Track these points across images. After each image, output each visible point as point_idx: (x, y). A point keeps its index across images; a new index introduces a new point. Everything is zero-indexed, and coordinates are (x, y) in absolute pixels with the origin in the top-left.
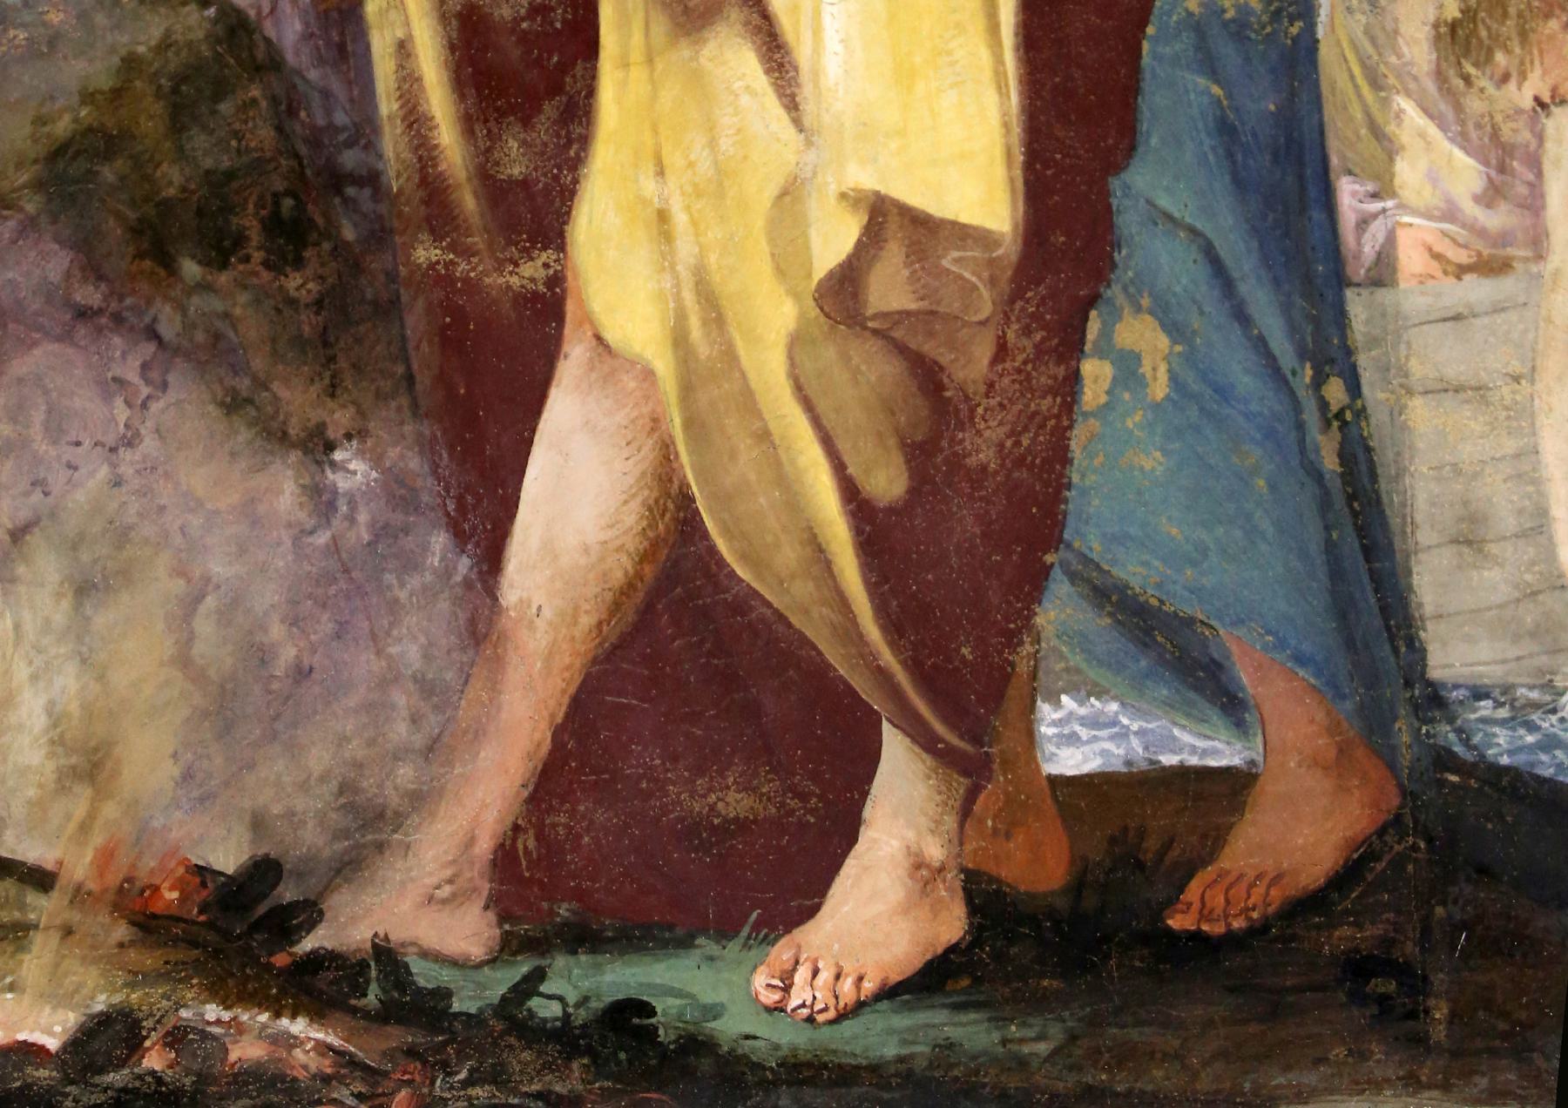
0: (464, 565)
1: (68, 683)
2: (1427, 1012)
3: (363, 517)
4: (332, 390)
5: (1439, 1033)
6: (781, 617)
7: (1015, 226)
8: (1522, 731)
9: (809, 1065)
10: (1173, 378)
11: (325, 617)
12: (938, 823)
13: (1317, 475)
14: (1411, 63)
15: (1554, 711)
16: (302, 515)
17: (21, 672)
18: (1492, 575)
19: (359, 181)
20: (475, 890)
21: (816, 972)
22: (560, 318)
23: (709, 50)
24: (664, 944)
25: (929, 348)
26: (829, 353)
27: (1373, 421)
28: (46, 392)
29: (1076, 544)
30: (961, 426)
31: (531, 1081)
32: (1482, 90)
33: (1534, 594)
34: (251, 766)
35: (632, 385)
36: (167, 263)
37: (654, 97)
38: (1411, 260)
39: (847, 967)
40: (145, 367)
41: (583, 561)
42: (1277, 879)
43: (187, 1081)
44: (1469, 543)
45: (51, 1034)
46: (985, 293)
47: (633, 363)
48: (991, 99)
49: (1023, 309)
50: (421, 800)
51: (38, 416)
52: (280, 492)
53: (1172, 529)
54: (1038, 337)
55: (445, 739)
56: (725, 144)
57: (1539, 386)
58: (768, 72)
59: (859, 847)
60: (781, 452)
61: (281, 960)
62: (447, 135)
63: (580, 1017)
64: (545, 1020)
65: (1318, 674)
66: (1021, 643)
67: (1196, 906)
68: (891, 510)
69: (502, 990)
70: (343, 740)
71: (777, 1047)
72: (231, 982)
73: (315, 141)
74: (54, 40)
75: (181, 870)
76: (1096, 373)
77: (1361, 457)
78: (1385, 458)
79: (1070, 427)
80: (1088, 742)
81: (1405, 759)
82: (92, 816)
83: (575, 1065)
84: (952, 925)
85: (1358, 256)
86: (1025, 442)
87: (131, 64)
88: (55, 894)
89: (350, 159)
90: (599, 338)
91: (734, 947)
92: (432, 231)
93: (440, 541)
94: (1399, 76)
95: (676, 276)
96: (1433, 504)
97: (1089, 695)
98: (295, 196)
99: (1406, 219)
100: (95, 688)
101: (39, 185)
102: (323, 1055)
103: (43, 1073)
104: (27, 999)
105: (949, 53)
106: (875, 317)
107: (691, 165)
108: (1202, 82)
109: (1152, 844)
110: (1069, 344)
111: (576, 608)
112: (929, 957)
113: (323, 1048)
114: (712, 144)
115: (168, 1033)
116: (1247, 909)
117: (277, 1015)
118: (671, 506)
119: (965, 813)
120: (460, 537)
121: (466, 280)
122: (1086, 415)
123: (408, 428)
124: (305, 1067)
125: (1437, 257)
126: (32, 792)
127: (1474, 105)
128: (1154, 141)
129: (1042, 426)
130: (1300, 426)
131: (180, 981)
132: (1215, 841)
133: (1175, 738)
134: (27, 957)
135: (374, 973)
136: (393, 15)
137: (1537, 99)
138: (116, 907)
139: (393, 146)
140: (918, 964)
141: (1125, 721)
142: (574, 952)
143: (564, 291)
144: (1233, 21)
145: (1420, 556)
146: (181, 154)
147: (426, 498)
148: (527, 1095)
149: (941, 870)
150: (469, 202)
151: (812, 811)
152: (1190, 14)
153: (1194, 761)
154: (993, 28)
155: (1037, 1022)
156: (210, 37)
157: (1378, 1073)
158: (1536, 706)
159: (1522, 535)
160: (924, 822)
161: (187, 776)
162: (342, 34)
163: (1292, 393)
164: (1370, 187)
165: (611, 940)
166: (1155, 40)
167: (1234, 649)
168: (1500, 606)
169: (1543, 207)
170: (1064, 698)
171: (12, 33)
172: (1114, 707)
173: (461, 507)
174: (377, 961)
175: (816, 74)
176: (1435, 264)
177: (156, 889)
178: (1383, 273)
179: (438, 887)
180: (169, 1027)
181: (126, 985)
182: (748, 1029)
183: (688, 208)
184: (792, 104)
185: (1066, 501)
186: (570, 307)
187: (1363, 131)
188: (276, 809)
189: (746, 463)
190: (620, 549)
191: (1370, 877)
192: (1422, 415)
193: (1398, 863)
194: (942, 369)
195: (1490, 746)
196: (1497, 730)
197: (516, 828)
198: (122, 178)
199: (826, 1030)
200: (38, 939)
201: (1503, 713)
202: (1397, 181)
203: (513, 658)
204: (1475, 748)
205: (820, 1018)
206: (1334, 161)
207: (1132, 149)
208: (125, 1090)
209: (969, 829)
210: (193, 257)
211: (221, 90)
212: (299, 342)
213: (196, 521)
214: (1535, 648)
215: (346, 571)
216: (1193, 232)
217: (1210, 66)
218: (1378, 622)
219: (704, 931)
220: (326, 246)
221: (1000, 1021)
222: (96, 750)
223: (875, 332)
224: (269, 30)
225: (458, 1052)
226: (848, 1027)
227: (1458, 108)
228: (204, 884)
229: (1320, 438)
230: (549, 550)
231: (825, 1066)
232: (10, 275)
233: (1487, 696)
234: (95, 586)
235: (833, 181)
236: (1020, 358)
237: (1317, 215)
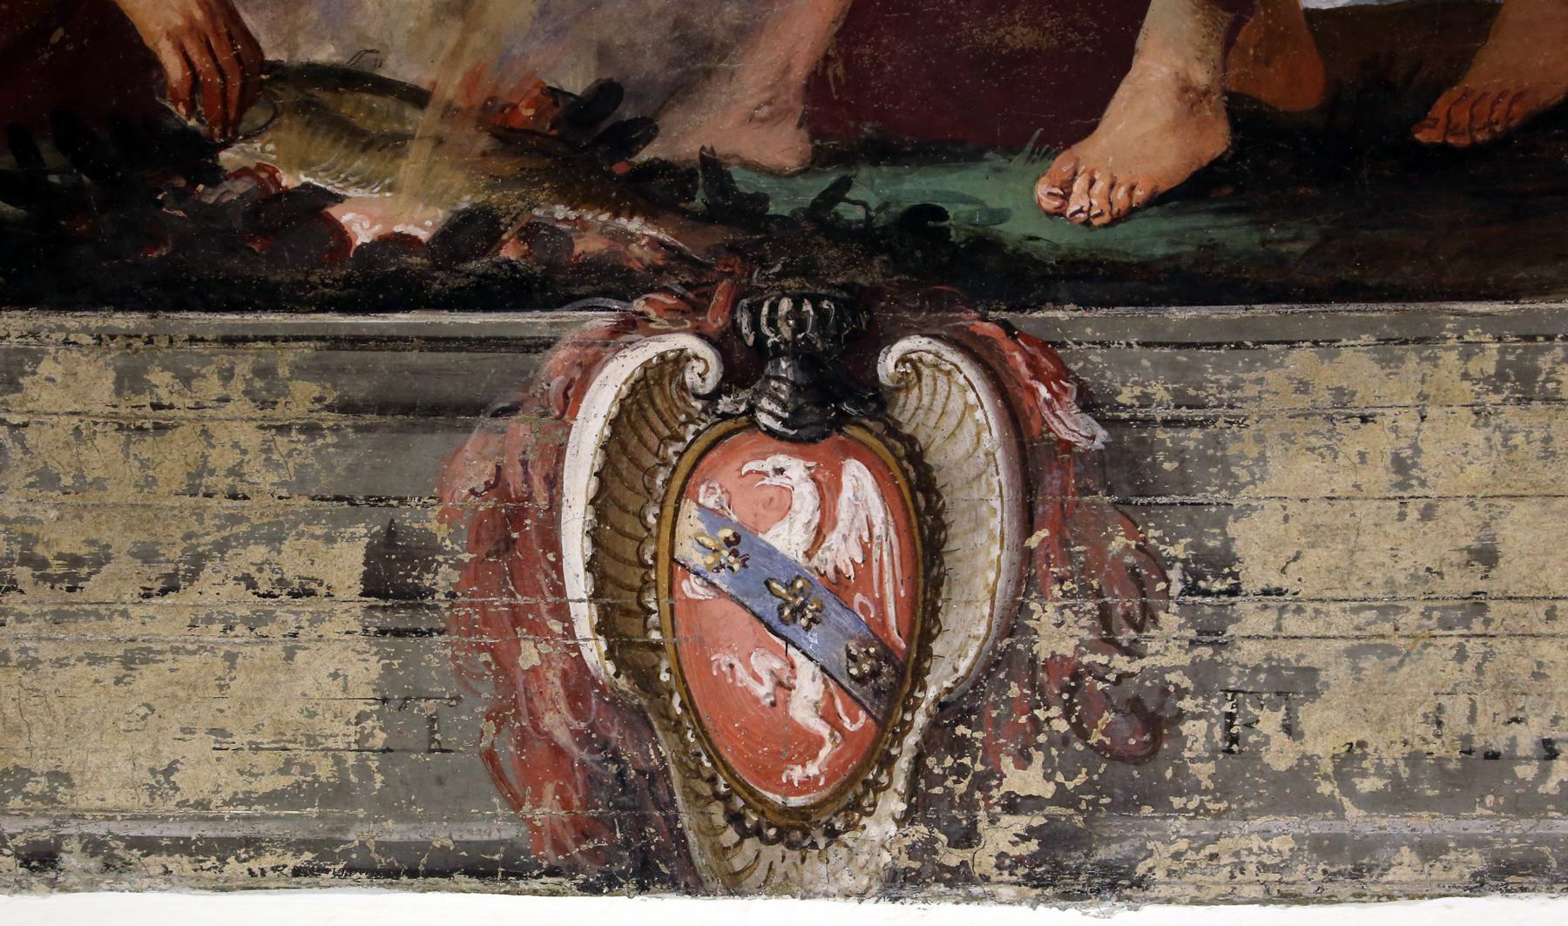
9: (1085, 262)
12: (1204, 52)
20: (789, 111)
21: (1092, 182)
24: (956, 158)
31: (837, 275)
39: (1121, 177)
42: (1519, 96)
43: (538, 269)
45: (423, 227)
50: (744, 33)
59: (1133, 73)
61: (620, 168)
63: (882, 219)
64: (850, 222)
67: (1443, 121)
69: (812, 196)
71: (1057, 247)
75: (537, 92)
82: (461, 44)
83: (876, 262)
84: (1215, 141)
88: (429, 111)
91: (1018, 161)
102: (655, 250)
103: (416, 260)
104: (403, 198)
112: (1195, 168)
113: (656, 244)
115: (523, 229)
116: (1490, 124)
117: (616, 215)
119: (1229, 43)
124: (640, 260)
131: (534, 184)
134: (404, 163)
135: (701, 181)
140: (1184, 175)
142: (876, 164)
148: (834, 286)
149: (1206, 93)
160: (1190, 51)
174: (704, 170)
177: (515, 107)
179: (759, 108)
180: (523, 223)
181: (487, 187)
182: (1031, 231)
188: (619, 41)
197: (827, 58)
199: (1102, 233)
200: (414, 148)
205: (1096, 222)
208: (485, 276)
209: (1232, 59)
225: (773, 249)
226: (1122, 229)
228: (556, 104)
231: (1100, 264)
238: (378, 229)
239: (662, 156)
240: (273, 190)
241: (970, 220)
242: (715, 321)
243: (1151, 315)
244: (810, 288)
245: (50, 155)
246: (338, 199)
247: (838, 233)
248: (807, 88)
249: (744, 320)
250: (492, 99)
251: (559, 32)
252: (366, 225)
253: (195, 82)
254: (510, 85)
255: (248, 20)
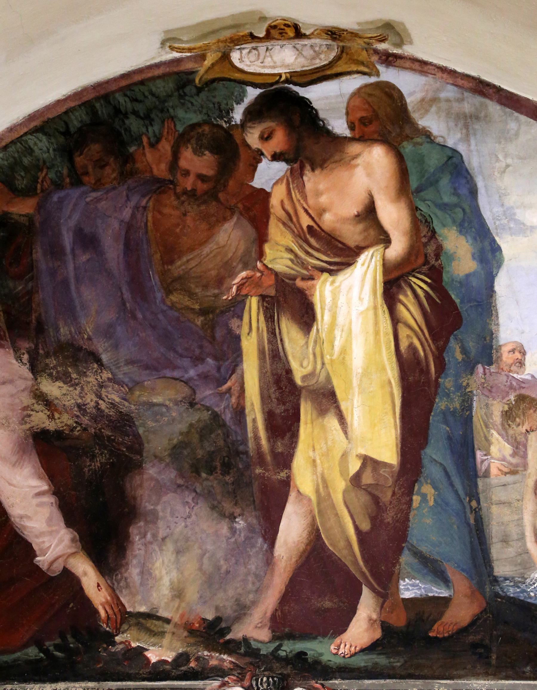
0: (266, 546)
1: (174, 574)
2: (491, 657)
3: (242, 535)
4: (236, 504)
5: (494, 662)
6: (339, 559)
7: (398, 463)
8: (516, 588)
9: (343, 668)
10: (435, 500)
11: (233, 559)
12: (375, 609)
13: (468, 524)
14: (495, 422)
15: (524, 583)
16: (228, 534)
17: (164, 572)
18: (510, 549)
19: (243, 453)
20: (266, 625)
21: (345, 645)
22: (289, 486)
23: (326, 419)
25: (377, 493)
26: (353, 494)
27: (483, 511)
28: (170, 505)
29: (410, 541)
30: (383, 513)
32: (513, 428)
33: (521, 554)
34: (215, 594)
35: (306, 502)
36: (198, 473)
37: (313, 432)
38: (494, 471)
39: (353, 644)
40: (193, 499)
41: (293, 545)
42: (456, 624)
43: (200, 669)
44: (505, 542)
45: (169, 657)
46: (391, 479)
47: (306, 497)
48: (393, 431)
49: (399, 483)
50: (254, 603)
51: (169, 510)
52: (223, 529)
53: (434, 538)
54: (403, 490)
55: (260, 588)
56: (329, 443)
57: (524, 502)
58: (340, 425)
59: (356, 615)
60: (341, 519)
61: (221, 641)
62: (264, 442)
63: (290, 655)
64: (282, 656)
65: (467, 573)
66: (396, 566)
67: (436, 630)
68: (366, 533)
70: (236, 588)
71: (336, 663)
72: (210, 646)
73: (233, 443)
74: (174, 420)
75: (199, 619)
76: (416, 499)
77: (480, 520)
78: (485, 520)
79: (410, 512)
80: (412, 590)
81: (488, 595)
82: (179, 606)
83: (289, 667)
84: (378, 634)
85: (481, 470)
86: (399, 516)
87: (191, 425)
88: (171, 625)
89: (241, 448)
90: (298, 491)
91: (326, 639)
92: (260, 466)
93: (260, 540)
94: (492, 425)
95: (317, 476)
96: (497, 532)
97: (412, 579)
98: (228, 457)
99: (493, 461)
100: (180, 576)
101: (170, 455)
102: (230, 664)
103: (168, 667)
104: (164, 649)
105: (383, 420)
106: (363, 486)
107: (321, 448)
108: (444, 426)
109: (426, 615)
110: (410, 492)
111: (291, 557)
112: (372, 642)
113: (231, 662)
114: (326, 443)
116: (448, 632)
117: (220, 654)
118: (314, 532)
119: (382, 607)
120: (265, 539)
121: (268, 477)
122: (413, 509)
123: (253, 513)
124: (227, 667)
125: (500, 470)
126: (166, 600)
127: (511, 432)
128: (432, 441)
129: (403, 512)
130: (465, 512)
131: (198, 645)
132: (441, 614)
133: (432, 589)
136: (252, 412)
137: (526, 430)
138: (185, 628)
139: (251, 444)
140: (370, 644)
141: (420, 585)
142: (289, 640)
143: (290, 479)
144: (452, 411)
145: (494, 545)
146: (202, 447)
147: (257, 530)
149: (375, 621)
150: (269, 458)
151: (346, 606)
152: (442, 410)
153: (436, 595)
154: (394, 413)
155: (397, 658)
156: (210, 419)
157: (478, 671)
158: (520, 582)
159: (518, 540)
160: (372, 609)
161: (201, 597)
162: (240, 418)
163: (463, 504)
164: (484, 453)
165: (299, 637)
166: (433, 416)
167: (447, 567)
168: (512, 558)
169: (527, 458)
170: (406, 579)
171: (164, 418)
172: (418, 582)
173: (265, 532)
175: (352, 425)
176: (499, 472)
177: (193, 624)
178: (487, 474)
179: (258, 624)
181: (187, 646)
183: (320, 459)
184: (346, 433)
185: (408, 531)
186: (292, 483)
187: (483, 439)
188: (221, 605)
189: (332, 521)
190: (302, 542)
191: (478, 624)
192: (495, 509)
193: (485, 620)
194: (379, 498)
195: (508, 592)
196: (510, 588)
197: (276, 610)
198: (189, 454)
199: (348, 660)
201: (512, 584)
202: (491, 451)
203: (276, 569)
204: (505, 592)
205: (346, 656)
206: (476, 446)
207: (427, 443)
208: (186, 671)
209: (383, 611)
210: (204, 473)
211: (211, 431)
212: (228, 492)
213: (204, 536)
214: (520, 568)
215: (238, 548)
216: (441, 464)
217: (446, 422)
218: (482, 561)
219: (320, 635)
220: (235, 469)
221: (388, 658)
222: (180, 590)
223: (364, 489)
224: (223, 417)
225: (262, 663)
226: (353, 658)
227: (507, 433)
228: (204, 623)
229: (470, 515)
230: (285, 542)
231: (347, 668)
232: (163, 477)
233: (508, 580)
234: (180, 552)
235: (354, 453)
236: (398, 495)
237: (471, 460)
238: (158, 658)
239: (233, 637)
240: (129, 648)
241: (314, 656)
242: (246, 683)
243: (360, 682)
244: (271, 674)
245: (70, 639)
246: (147, 650)
247: (279, 659)
248: (271, 618)
249: (254, 683)
250: (188, 621)
251: (205, 602)
252: (154, 657)
253: (108, 618)
254: (192, 617)
255: (122, 599)
